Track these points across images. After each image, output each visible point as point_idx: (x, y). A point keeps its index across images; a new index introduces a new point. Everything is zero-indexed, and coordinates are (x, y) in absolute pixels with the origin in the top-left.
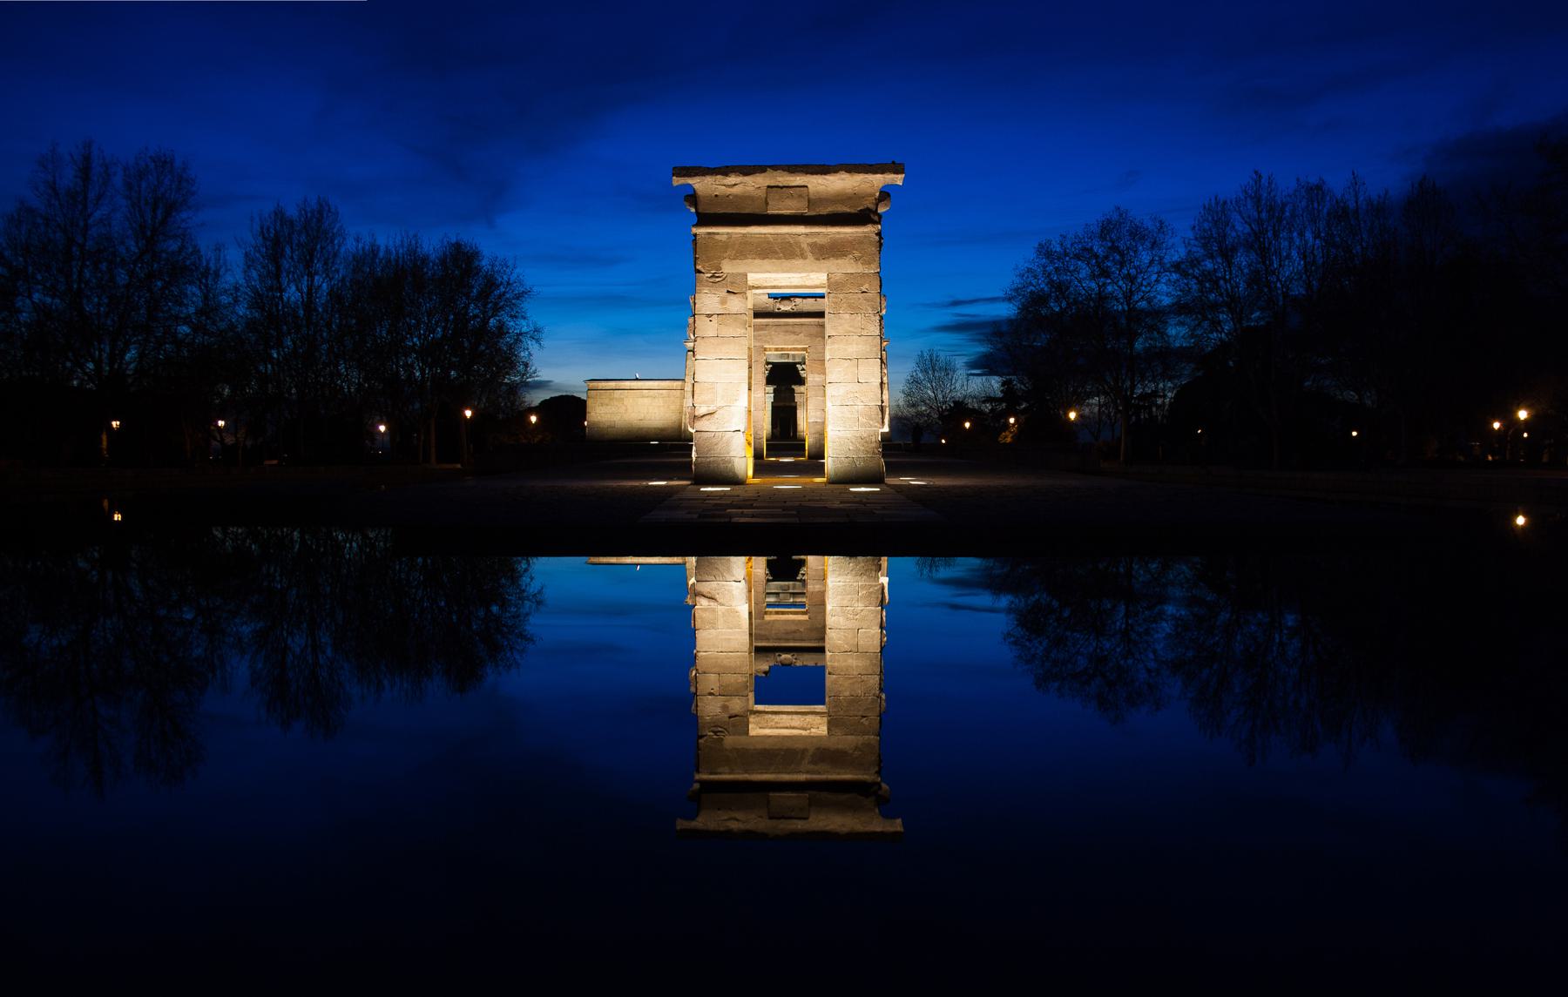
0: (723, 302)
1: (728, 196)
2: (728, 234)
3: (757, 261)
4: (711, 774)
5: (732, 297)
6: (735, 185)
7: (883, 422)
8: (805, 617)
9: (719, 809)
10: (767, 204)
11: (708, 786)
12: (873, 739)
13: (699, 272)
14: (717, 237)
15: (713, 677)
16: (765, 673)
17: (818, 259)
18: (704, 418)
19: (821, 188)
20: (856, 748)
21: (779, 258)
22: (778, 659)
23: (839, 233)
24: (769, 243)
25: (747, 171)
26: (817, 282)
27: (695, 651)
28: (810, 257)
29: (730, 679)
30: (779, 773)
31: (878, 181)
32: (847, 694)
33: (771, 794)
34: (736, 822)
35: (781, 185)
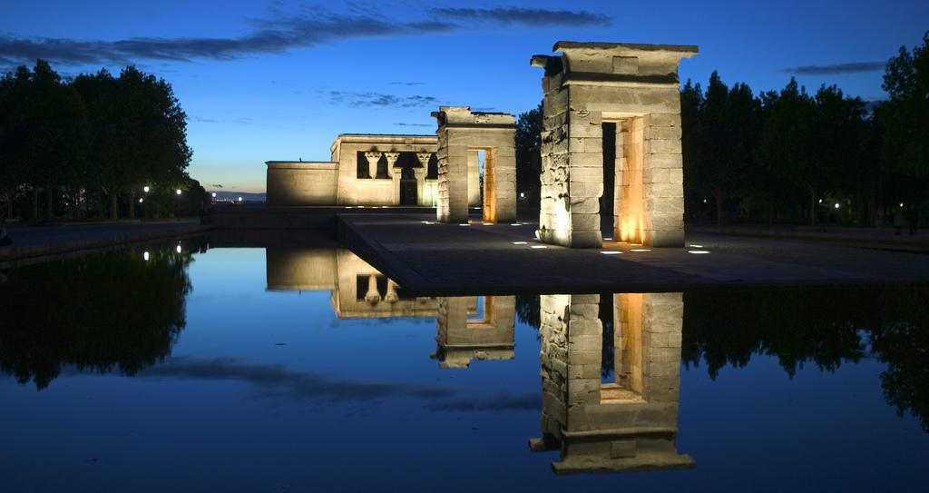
0: (588, 130)
2: (590, 86)
3: (608, 104)
4: (576, 431)
10: (613, 68)
12: (676, 404)
14: (583, 88)
15: (580, 367)
17: (644, 104)
19: (646, 59)
20: (665, 409)
25: (605, 46)
28: (640, 102)
29: (589, 368)
30: (618, 427)
31: (682, 54)
32: (661, 375)
33: (613, 442)
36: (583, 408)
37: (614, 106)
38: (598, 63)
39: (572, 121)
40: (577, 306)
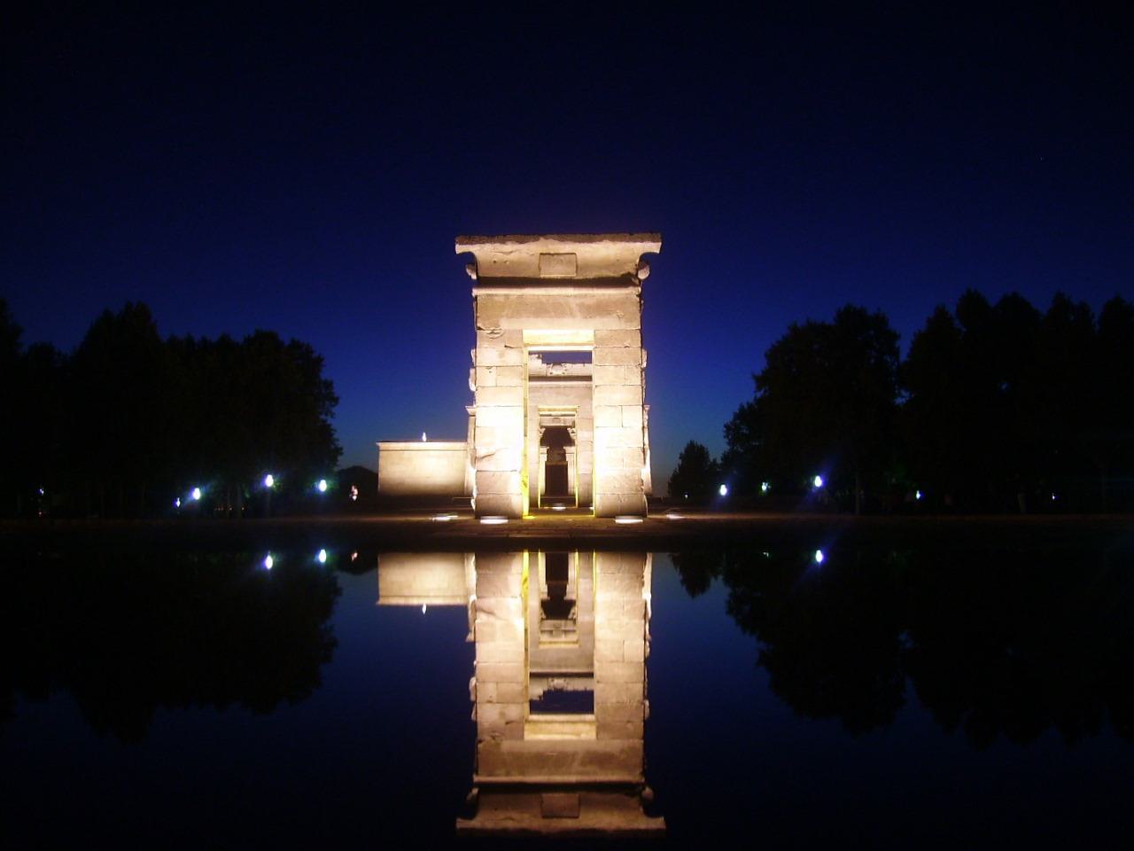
0: (501, 355)
1: (505, 262)
3: (532, 320)
5: (509, 351)
6: (511, 252)
7: (645, 459)
8: (576, 646)
9: (496, 809)
10: (540, 269)
11: (487, 788)
12: (638, 743)
13: (480, 329)
14: (496, 298)
16: (540, 697)
17: (586, 318)
18: (484, 460)
20: (622, 751)
21: (551, 317)
22: (552, 684)
23: (604, 295)
24: (541, 303)
26: (585, 340)
27: (475, 663)
28: (579, 314)
29: (506, 687)
30: (552, 774)
32: (614, 700)
33: (544, 795)
34: (511, 822)
35: (552, 252)
36: (498, 745)
37: (539, 322)
38: (518, 264)
39: (478, 343)
40: (483, 600)
